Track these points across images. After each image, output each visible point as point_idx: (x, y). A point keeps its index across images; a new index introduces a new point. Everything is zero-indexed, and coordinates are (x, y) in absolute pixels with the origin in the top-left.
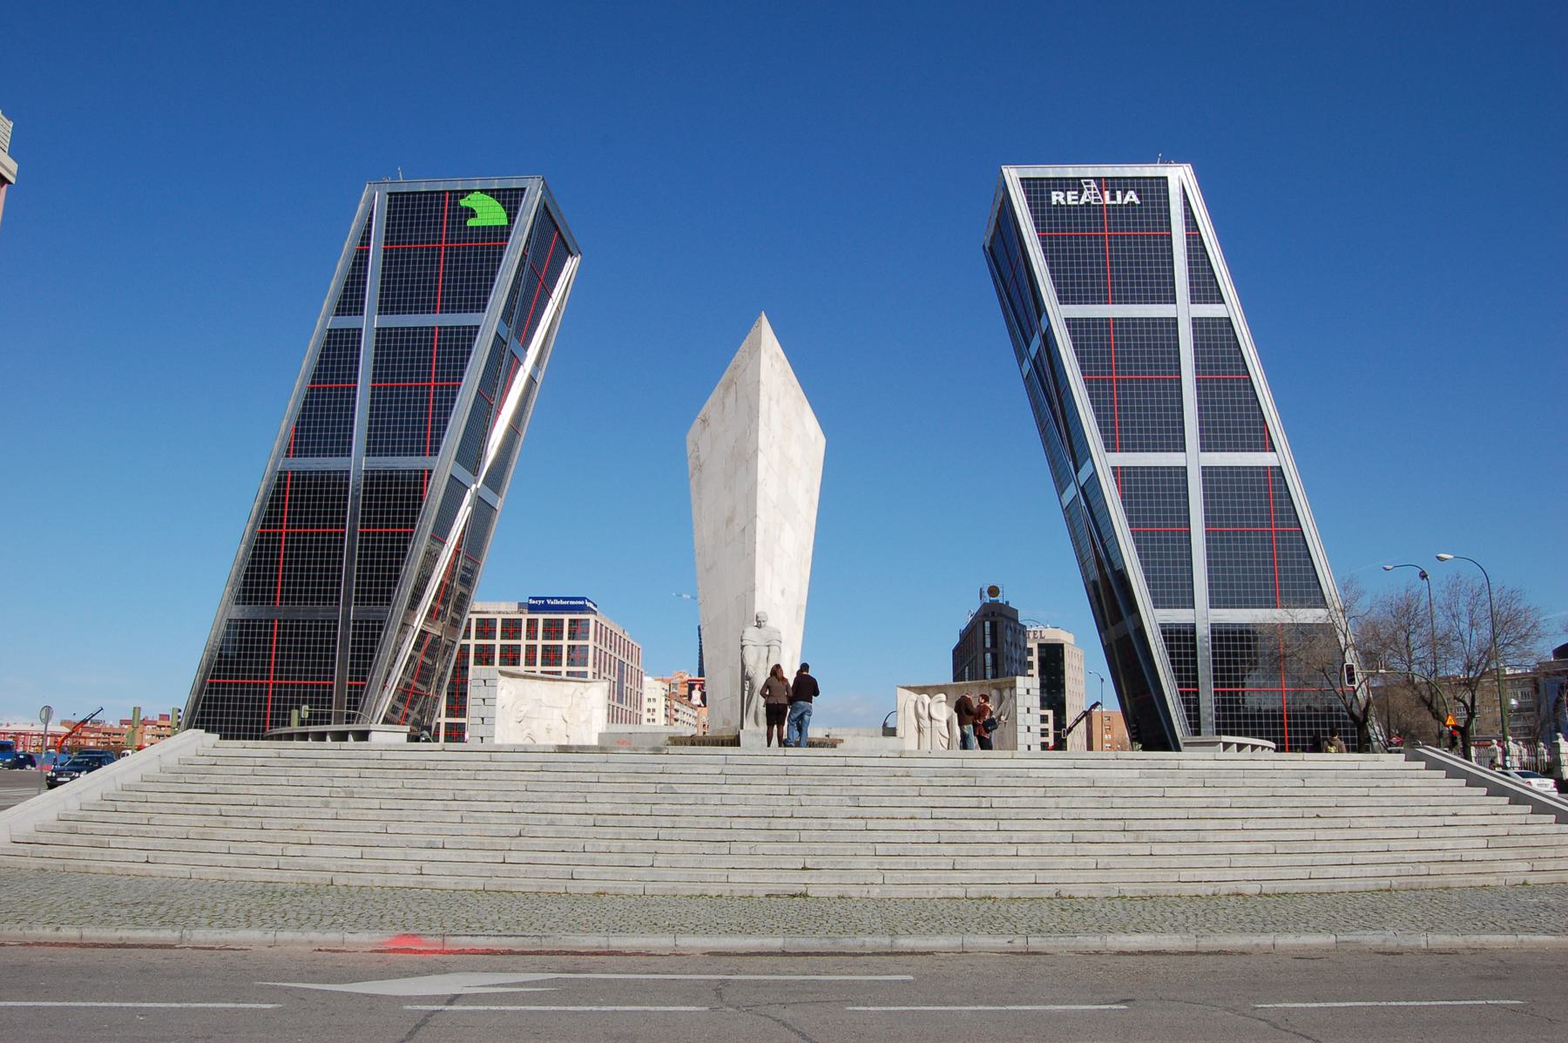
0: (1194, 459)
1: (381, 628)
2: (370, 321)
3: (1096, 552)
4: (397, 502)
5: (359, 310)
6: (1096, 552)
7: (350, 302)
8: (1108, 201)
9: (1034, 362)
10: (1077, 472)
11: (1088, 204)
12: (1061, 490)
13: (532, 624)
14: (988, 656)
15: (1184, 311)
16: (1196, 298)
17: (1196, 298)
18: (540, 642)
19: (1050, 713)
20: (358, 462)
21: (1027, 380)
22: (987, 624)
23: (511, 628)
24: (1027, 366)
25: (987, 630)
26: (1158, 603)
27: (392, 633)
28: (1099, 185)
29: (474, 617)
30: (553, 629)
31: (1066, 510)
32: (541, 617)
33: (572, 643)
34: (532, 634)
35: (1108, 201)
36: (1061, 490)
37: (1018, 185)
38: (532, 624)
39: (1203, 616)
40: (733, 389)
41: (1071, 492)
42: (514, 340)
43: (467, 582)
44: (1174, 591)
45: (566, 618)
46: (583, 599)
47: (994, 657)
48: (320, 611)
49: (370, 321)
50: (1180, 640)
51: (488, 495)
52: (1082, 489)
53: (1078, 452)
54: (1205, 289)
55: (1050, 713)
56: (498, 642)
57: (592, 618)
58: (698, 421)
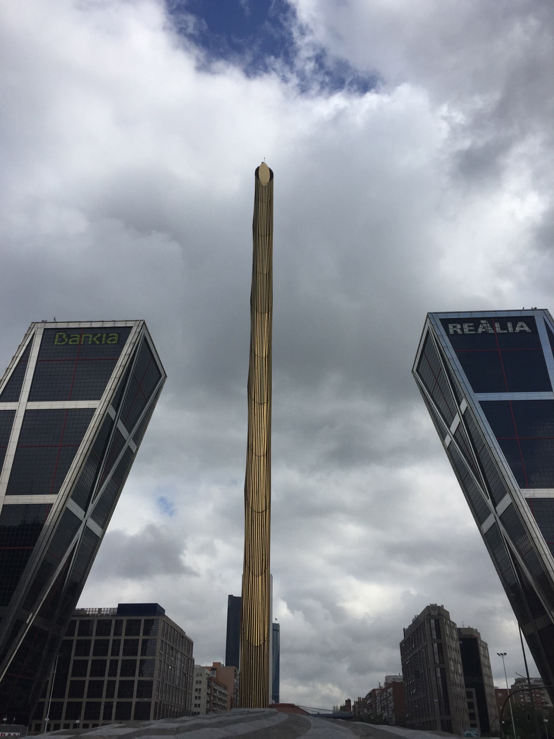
8: (498, 330)
9: (454, 436)
10: (495, 505)
13: (119, 623)
14: (436, 645)
19: (473, 690)
22: (433, 621)
25: (433, 625)
29: (78, 620)
30: (133, 628)
32: (125, 619)
33: (146, 637)
37: (439, 323)
38: (119, 623)
42: (120, 421)
43: (76, 589)
45: (143, 619)
46: (157, 604)
47: (440, 646)
52: (500, 518)
53: (498, 491)
55: (473, 690)
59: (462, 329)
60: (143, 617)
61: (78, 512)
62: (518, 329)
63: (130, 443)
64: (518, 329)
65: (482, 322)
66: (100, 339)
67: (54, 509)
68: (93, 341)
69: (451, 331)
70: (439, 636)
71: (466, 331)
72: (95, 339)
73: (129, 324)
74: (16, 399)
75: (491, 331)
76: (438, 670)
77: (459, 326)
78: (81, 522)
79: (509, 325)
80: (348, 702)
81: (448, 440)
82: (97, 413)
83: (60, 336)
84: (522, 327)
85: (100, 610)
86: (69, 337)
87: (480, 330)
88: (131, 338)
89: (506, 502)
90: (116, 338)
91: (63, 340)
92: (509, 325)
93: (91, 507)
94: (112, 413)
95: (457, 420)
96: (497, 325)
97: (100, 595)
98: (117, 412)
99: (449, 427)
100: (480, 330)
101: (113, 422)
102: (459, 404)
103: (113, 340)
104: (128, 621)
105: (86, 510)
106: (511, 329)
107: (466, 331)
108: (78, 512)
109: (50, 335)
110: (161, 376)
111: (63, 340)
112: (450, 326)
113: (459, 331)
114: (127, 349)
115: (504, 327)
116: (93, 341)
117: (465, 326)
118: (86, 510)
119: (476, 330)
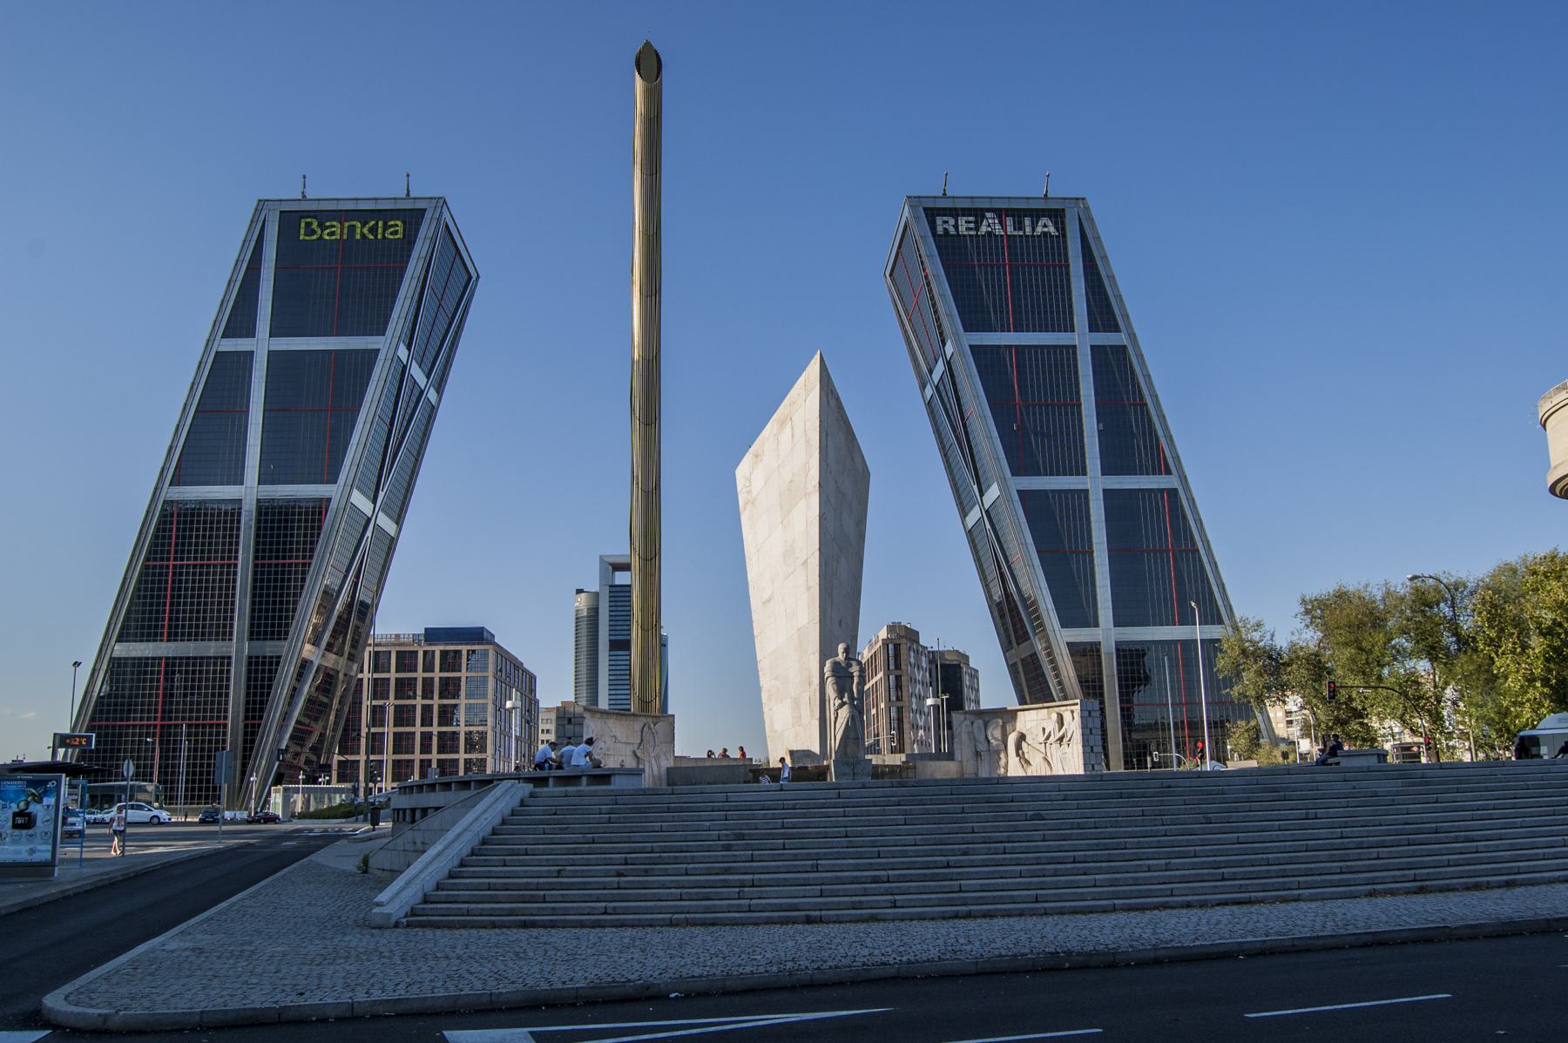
0: (1095, 482)
1: (278, 663)
2: (261, 344)
3: (1002, 574)
4: (288, 533)
5: (250, 333)
6: (1002, 574)
7: (239, 320)
8: (1010, 230)
10: (982, 495)
11: (989, 233)
12: (964, 514)
15: (1082, 338)
16: (1093, 328)
17: (1093, 328)
18: (437, 675)
20: (248, 491)
21: (929, 404)
23: (406, 660)
24: (929, 391)
26: (1065, 624)
27: (287, 672)
28: (1000, 217)
31: (969, 533)
32: (438, 649)
34: (428, 667)
35: (1010, 230)
36: (964, 514)
39: (1106, 633)
40: (788, 429)
41: (974, 515)
43: (364, 612)
44: (1076, 610)
45: (464, 649)
46: (483, 629)
48: (212, 648)
49: (261, 344)
50: (1085, 654)
51: (388, 525)
52: (987, 512)
54: (1104, 314)
56: (393, 675)
57: (490, 647)
58: (748, 458)
59: (956, 226)
60: (460, 643)
61: (365, 506)
62: (1039, 230)
63: (432, 395)
64: (1039, 230)
65: (988, 215)
66: (373, 230)
67: (333, 505)
68: (363, 235)
69: (940, 230)
70: (898, 667)
71: (962, 229)
72: (365, 231)
73: (419, 205)
74: (250, 333)
75: (999, 231)
76: (893, 709)
77: (952, 221)
78: (369, 520)
79: (1027, 221)
80: (710, 753)
81: (929, 391)
82: (381, 356)
83: (308, 225)
84: (1046, 226)
85: (397, 636)
86: (322, 226)
87: (984, 229)
88: (426, 231)
89: (993, 493)
90: (400, 229)
91: (314, 232)
92: (1027, 221)
93: (381, 495)
94: (403, 353)
95: (940, 368)
96: (1009, 221)
97: (398, 618)
98: (409, 348)
99: (931, 372)
100: (984, 229)
101: (405, 367)
102: (944, 344)
103: (396, 232)
104: (444, 654)
105: (374, 501)
106: (1028, 230)
107: (962, 229)
108: (365, 506)
109: (290, 220)
110: (470, 278)
111: (314, 232)
112: (939, 220)
113: (952, 231)
114: (420, 250)
115: (1019, 225)
116: (363, 235)
117: (962, 221)
118: (374, 501)
119: (977, 229)
